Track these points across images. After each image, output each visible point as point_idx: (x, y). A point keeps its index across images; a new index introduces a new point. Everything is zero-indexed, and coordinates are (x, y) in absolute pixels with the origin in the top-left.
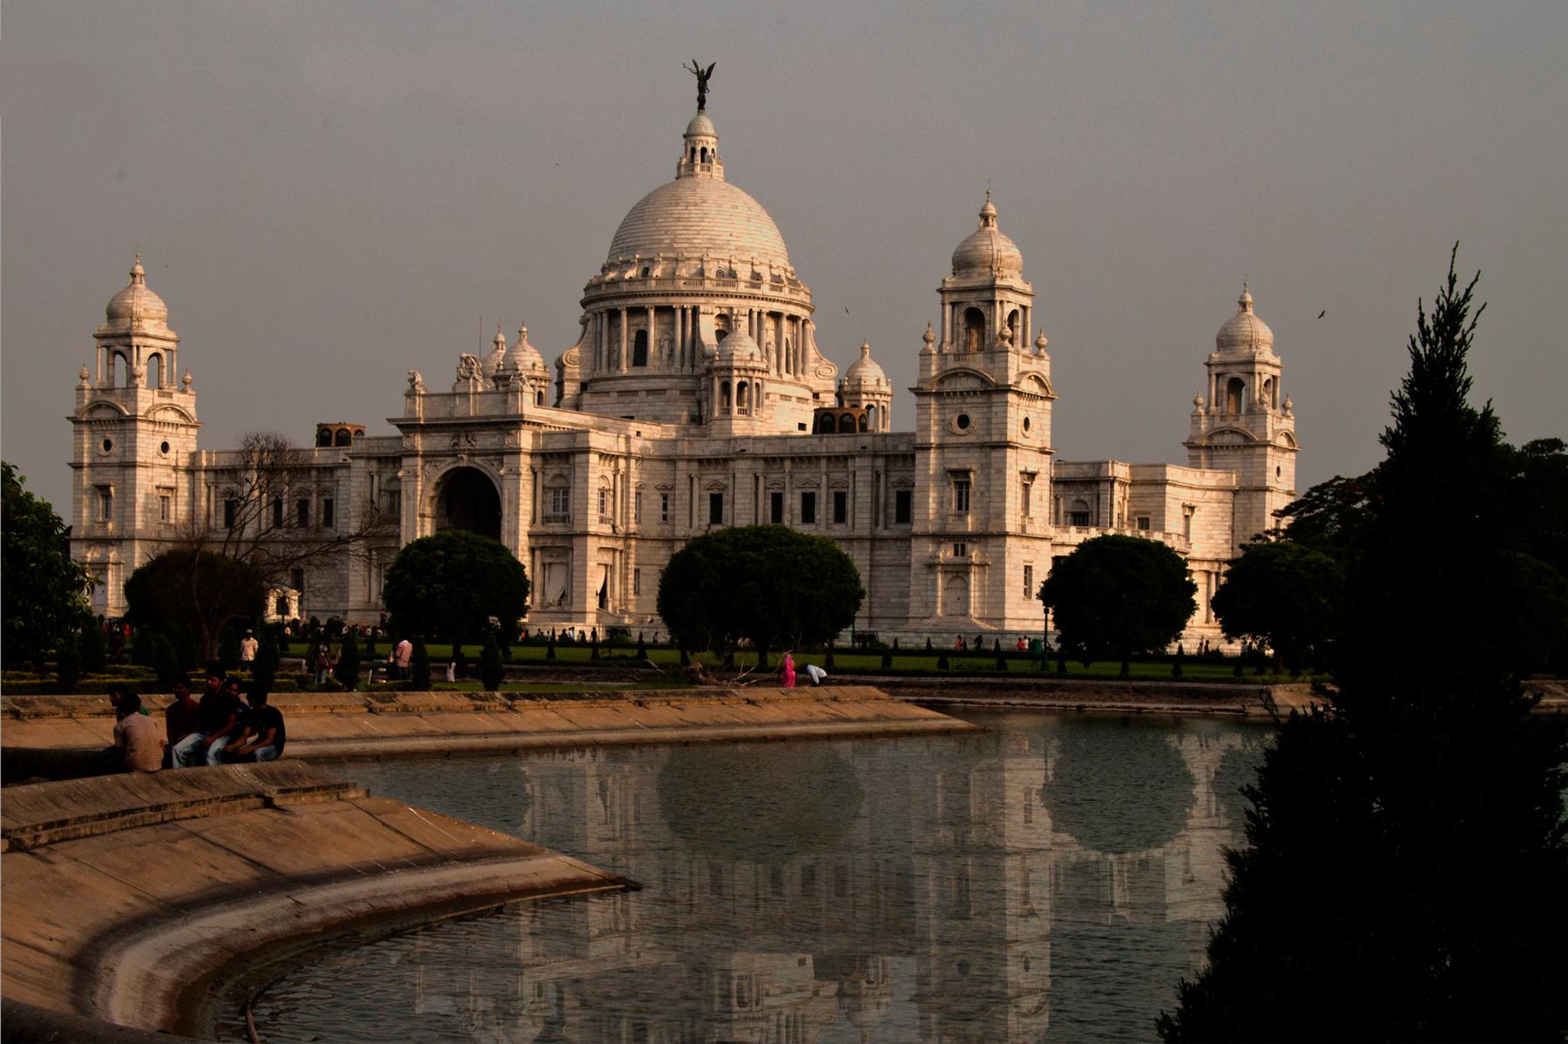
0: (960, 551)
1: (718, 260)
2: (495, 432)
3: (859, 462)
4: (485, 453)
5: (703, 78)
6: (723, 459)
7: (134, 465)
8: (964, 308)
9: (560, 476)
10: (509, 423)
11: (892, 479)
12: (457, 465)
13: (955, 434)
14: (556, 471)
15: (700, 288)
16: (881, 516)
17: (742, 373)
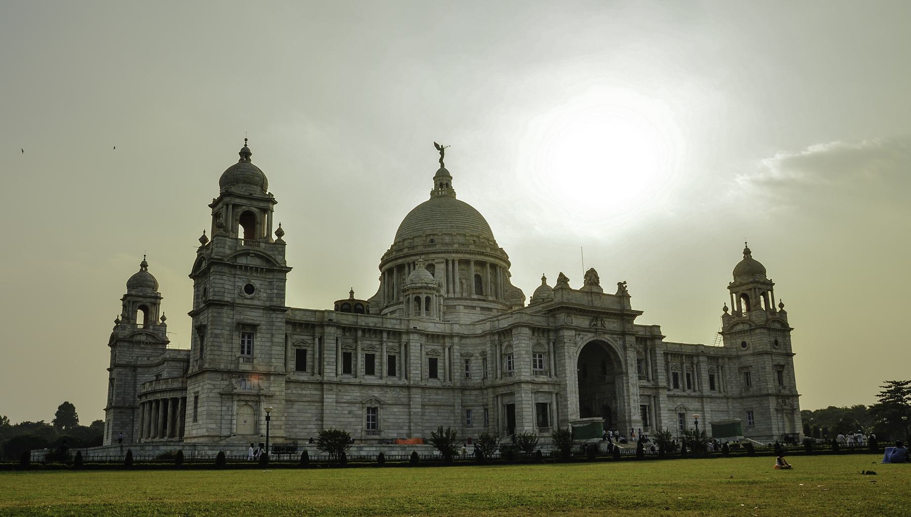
0: (784, 402)
3: (701, 358)
4: (612, 333)
12: (595, 339)
13: (775, 348)
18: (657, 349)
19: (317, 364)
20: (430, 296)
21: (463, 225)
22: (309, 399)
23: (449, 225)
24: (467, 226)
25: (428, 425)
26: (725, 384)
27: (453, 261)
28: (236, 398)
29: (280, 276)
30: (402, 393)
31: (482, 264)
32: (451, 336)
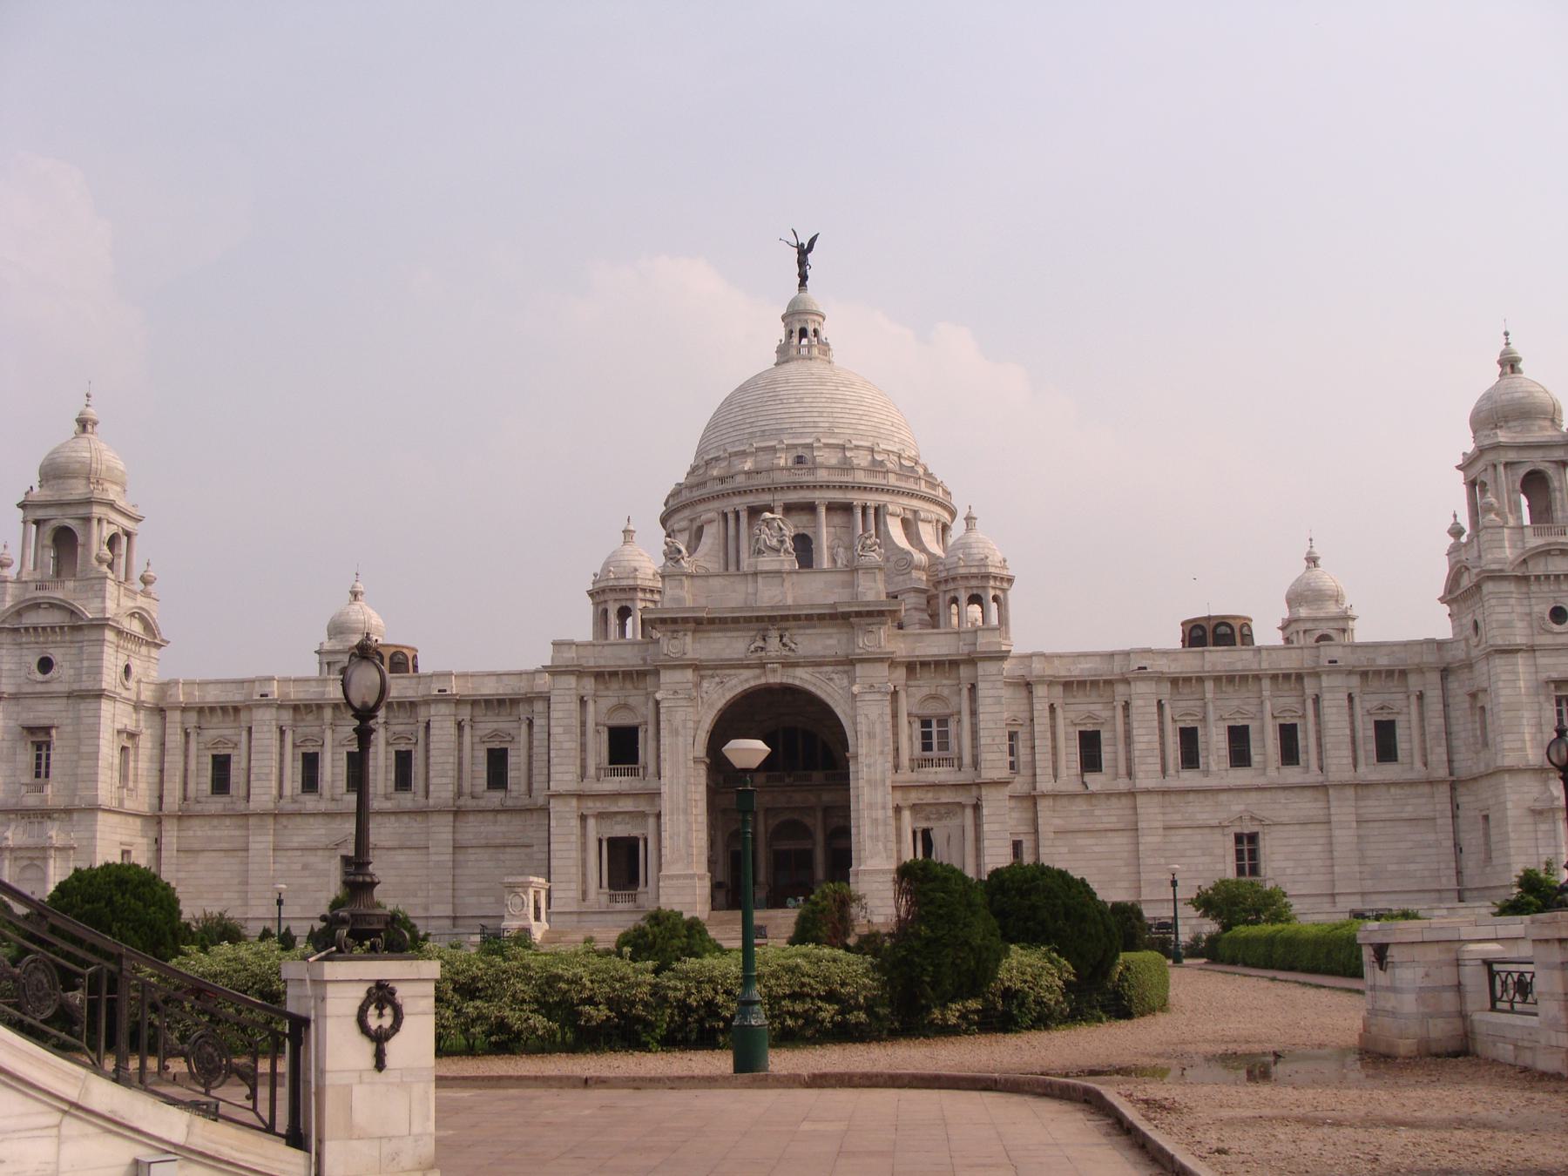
1: (888, 452)
2: (830, 631)
3: (1326, 681)
5: (803, 252)
6: (1106, 682)
7: (99, 695)
8: (1522, 471)
9: (933, 697)
10: (869, 614)
11: (1368, 706)
12: (763, 681)
13: (1551, 632)
14: (926, 691)
15: (885, 482)
16: (1361, 754)
17: (998, 584)
18: (981, 685)
19: (243, 780)
20: (629, 604)
21: (778, 427)
22: (225, 846)
23: (747, 431)
24: (788, 426)
25: (473, 886)
26: (1428, 746)
27: (737, 514)
28: (7, 854)
29: (94, 635)
30: (415, 825)
31: (810, 508)
32: (529, 700)
